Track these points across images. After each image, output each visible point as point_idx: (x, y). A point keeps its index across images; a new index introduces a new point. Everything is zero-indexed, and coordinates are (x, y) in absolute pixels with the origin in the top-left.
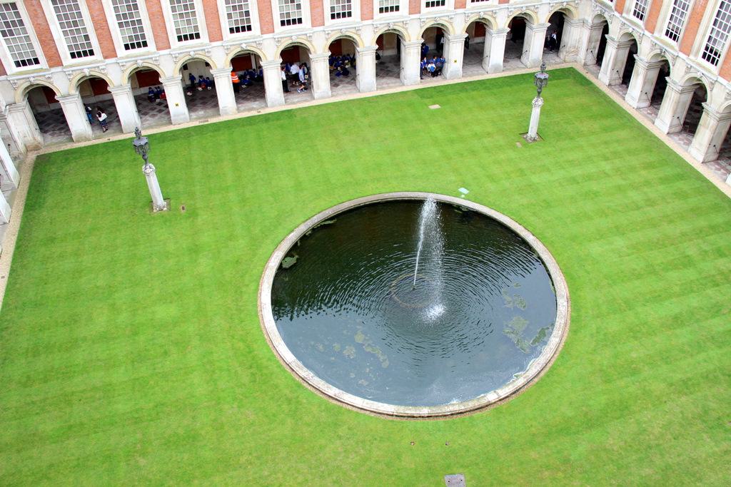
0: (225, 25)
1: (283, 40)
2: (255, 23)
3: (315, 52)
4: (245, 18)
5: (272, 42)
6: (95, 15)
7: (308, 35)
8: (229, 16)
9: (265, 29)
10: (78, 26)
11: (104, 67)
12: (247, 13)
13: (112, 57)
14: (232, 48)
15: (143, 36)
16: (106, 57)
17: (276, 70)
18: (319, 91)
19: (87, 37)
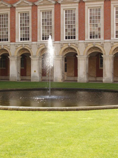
0: (63, 34)
1: (89, 45)
2: (77, 35)
3: (105, 54)
4: (73, 32)
5: (83, 44)
6: (12, 22)
7: (101, 43)
8: (66, 30)
9: (81, 38)
10: (5, 27)
11: (9, 45)
12: (74, 30)
13: (13, 42)
14: (64, 45)
15: (29, 36)
16: (11, 42)
17: (84, 61)
18: (105, 78)
19: (7, 32)
